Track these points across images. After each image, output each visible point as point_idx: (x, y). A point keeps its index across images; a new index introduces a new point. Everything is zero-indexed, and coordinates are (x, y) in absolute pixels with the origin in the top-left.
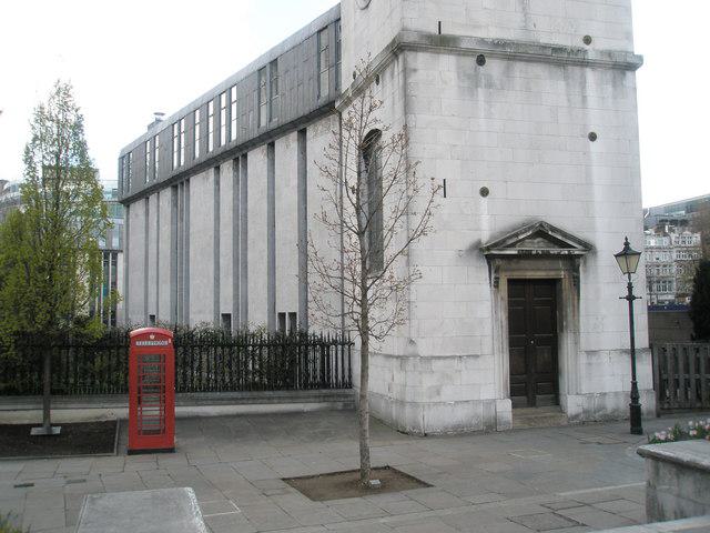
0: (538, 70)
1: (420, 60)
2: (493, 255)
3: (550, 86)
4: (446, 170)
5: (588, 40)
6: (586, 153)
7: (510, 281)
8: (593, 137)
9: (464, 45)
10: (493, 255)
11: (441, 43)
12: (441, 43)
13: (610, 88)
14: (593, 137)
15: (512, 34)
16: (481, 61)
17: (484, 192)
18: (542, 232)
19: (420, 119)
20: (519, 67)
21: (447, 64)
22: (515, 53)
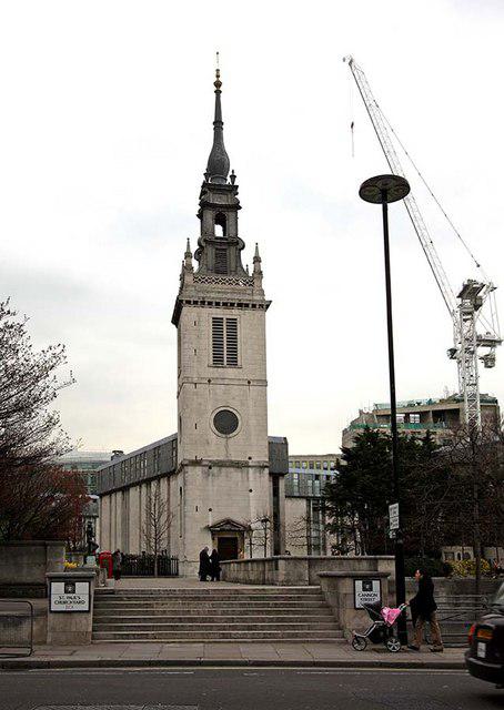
0: (232, 469)
1: (189, 469)
2: (213, 530)
3: (236, 475)
4: (198, 503)
5: (250, 458)
7: (219, 539)
8: (251, 491)
9: (204, 463)
10: (213, 530)
11: (197, 463)
12: (197, 463)
14: (251, 491)
16: (210, 468)
17: (210, 510)
18: (228, 522)
19: (189, 487)
20: (224, 469)
21: (198, 470)
22: (221, 464)
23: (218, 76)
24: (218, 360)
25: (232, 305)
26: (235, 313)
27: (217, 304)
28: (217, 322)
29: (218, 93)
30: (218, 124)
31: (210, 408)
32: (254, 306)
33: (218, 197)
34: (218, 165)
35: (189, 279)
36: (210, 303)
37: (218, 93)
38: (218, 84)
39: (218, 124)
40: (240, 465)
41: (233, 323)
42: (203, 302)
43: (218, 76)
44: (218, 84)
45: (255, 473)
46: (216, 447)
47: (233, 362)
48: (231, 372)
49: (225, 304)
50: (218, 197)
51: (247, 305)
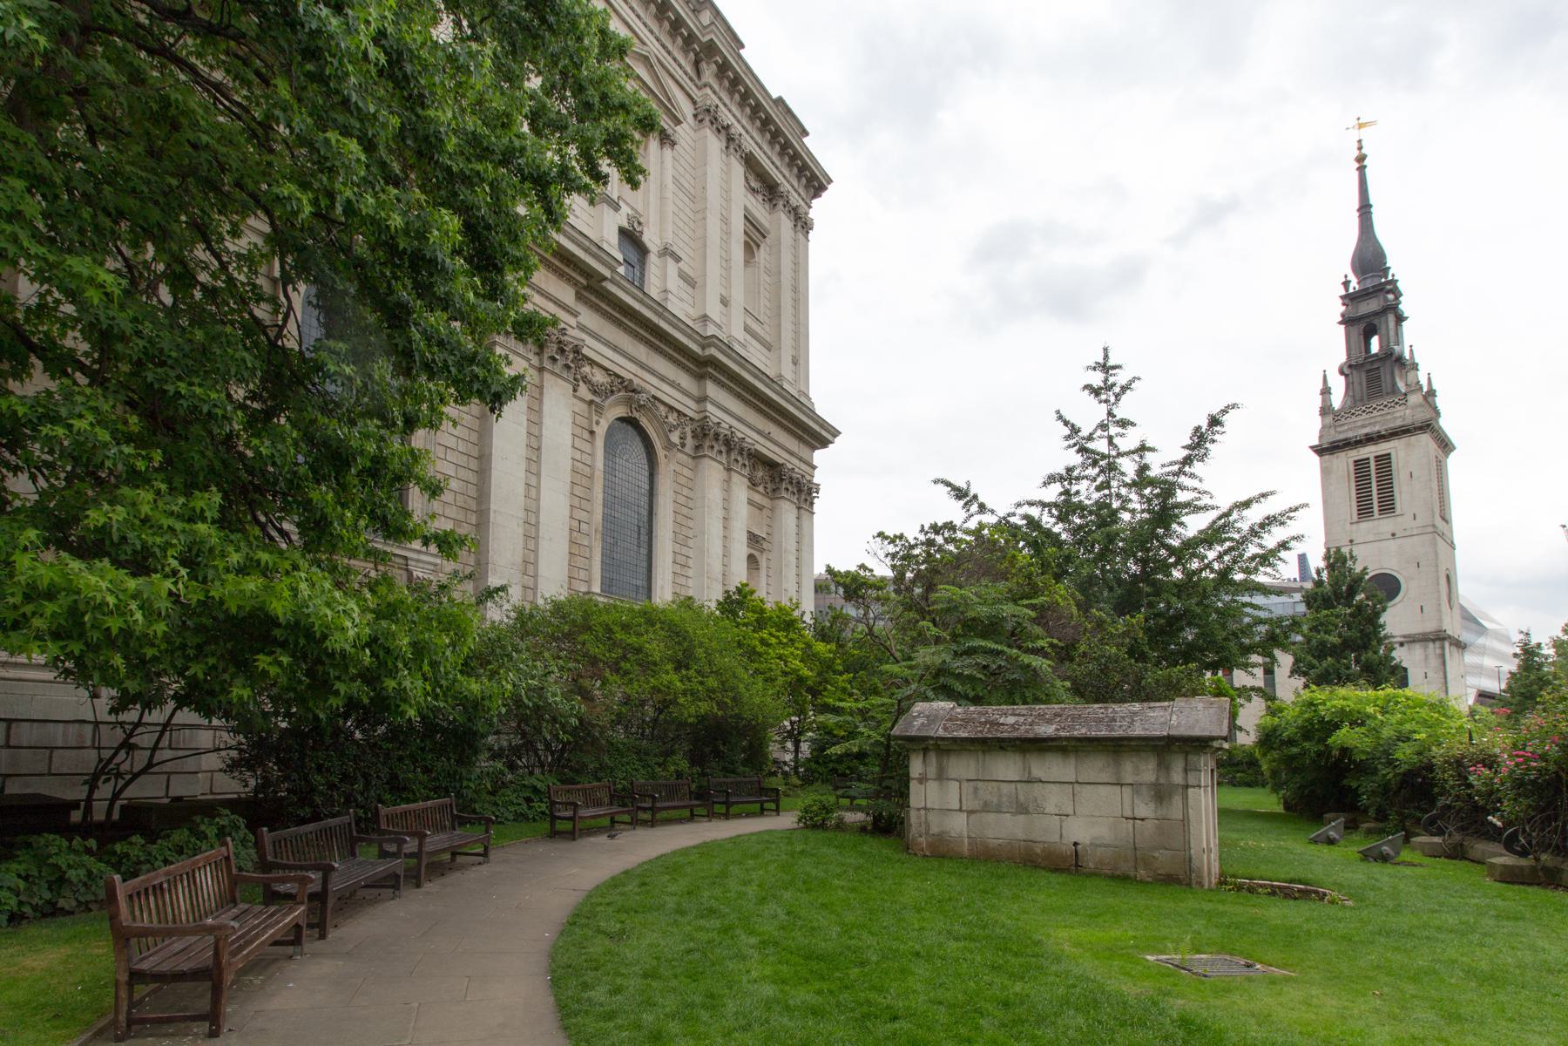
23: (1360, 148)
24: (1364, 511)
28: (1361, 465)
29: (1362, 170)
30: (1365, 209)
33: (1372, 305)
34: (1369, 260)
35: (1329, 419)
37: (1362, 170)
38: (1361, 159)
39: (1365, 209)
43: (1360, 148)
44: (1361, 159)
47: (1388, 506)
50: (1372, 305)
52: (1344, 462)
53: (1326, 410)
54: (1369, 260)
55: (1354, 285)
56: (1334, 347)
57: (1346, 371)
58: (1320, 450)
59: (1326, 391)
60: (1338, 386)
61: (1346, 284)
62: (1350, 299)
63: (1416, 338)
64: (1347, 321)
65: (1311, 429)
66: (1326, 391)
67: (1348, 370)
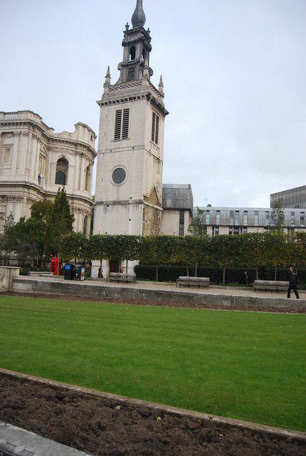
0: (120, 206)
3: (121, 209)
6: (128, 223)
11: (101, 203)
12: (101, 203)
13: (135, 209)
15: (115, 199)
24: (117, 137)
25: (126, 100)
26: (127, 105)
27: (118, 101)
28: (118, 113)
31: (111, 168)
32: (139, 98)
33: (137, 41)
34: (138, 19)
36: (114, 102)
40: (124, 204)
41: (127, 111)
42: (110, 102)
45: (133, 208)
46: (111, 193)
47: (125, 136)
48: (123, 143)
49: (122, 101)
51: (135, 98)
52: (113, 109)
53: (107, 85)
54: (138, 19)
55: (131, 27)
56: (118, 55)
57: (121, 68)
58: (101, 104)
59: (108, 76)
60: (116, 76)
61: (127, 26)
62: (128, 33)
63: (154, 60)
64: (124, 44)
65: (99, 92)
66: (108, 76)
67: (122, 66)
